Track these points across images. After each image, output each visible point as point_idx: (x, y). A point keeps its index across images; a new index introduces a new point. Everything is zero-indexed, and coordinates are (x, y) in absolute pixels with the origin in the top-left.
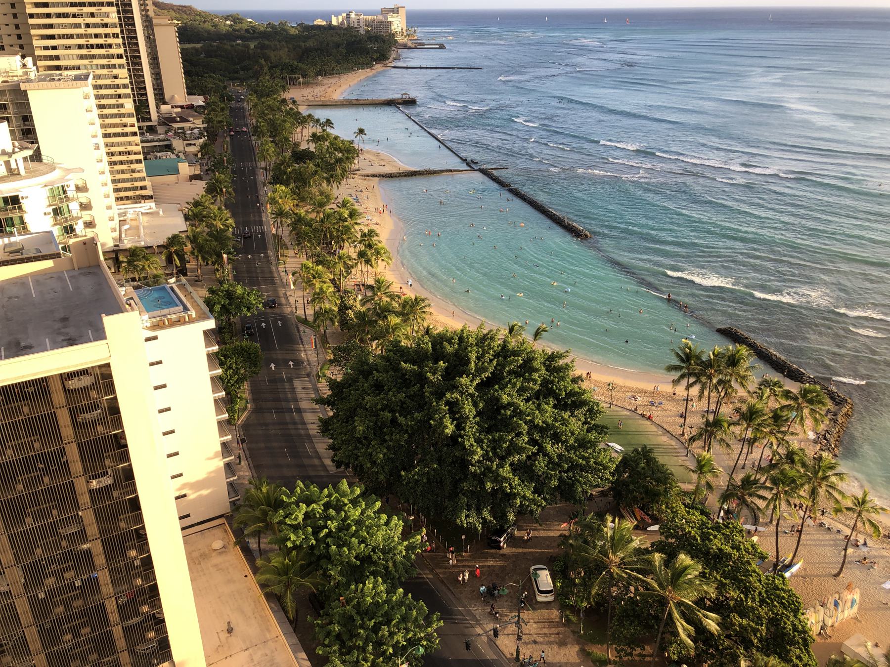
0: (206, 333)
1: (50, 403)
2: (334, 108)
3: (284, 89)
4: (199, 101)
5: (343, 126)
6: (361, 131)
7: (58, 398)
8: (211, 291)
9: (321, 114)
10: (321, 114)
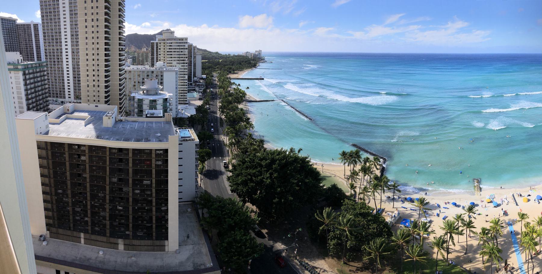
0: (196, 145)
1: (151, 156)
2: (242, 81)
3: (228, 74)
4: (204, 76)
5: (243, 86)
6: (248, 88)
7: (154, 156)
8: (200, 133)
9: (237, 82)
10: (237, 82)
